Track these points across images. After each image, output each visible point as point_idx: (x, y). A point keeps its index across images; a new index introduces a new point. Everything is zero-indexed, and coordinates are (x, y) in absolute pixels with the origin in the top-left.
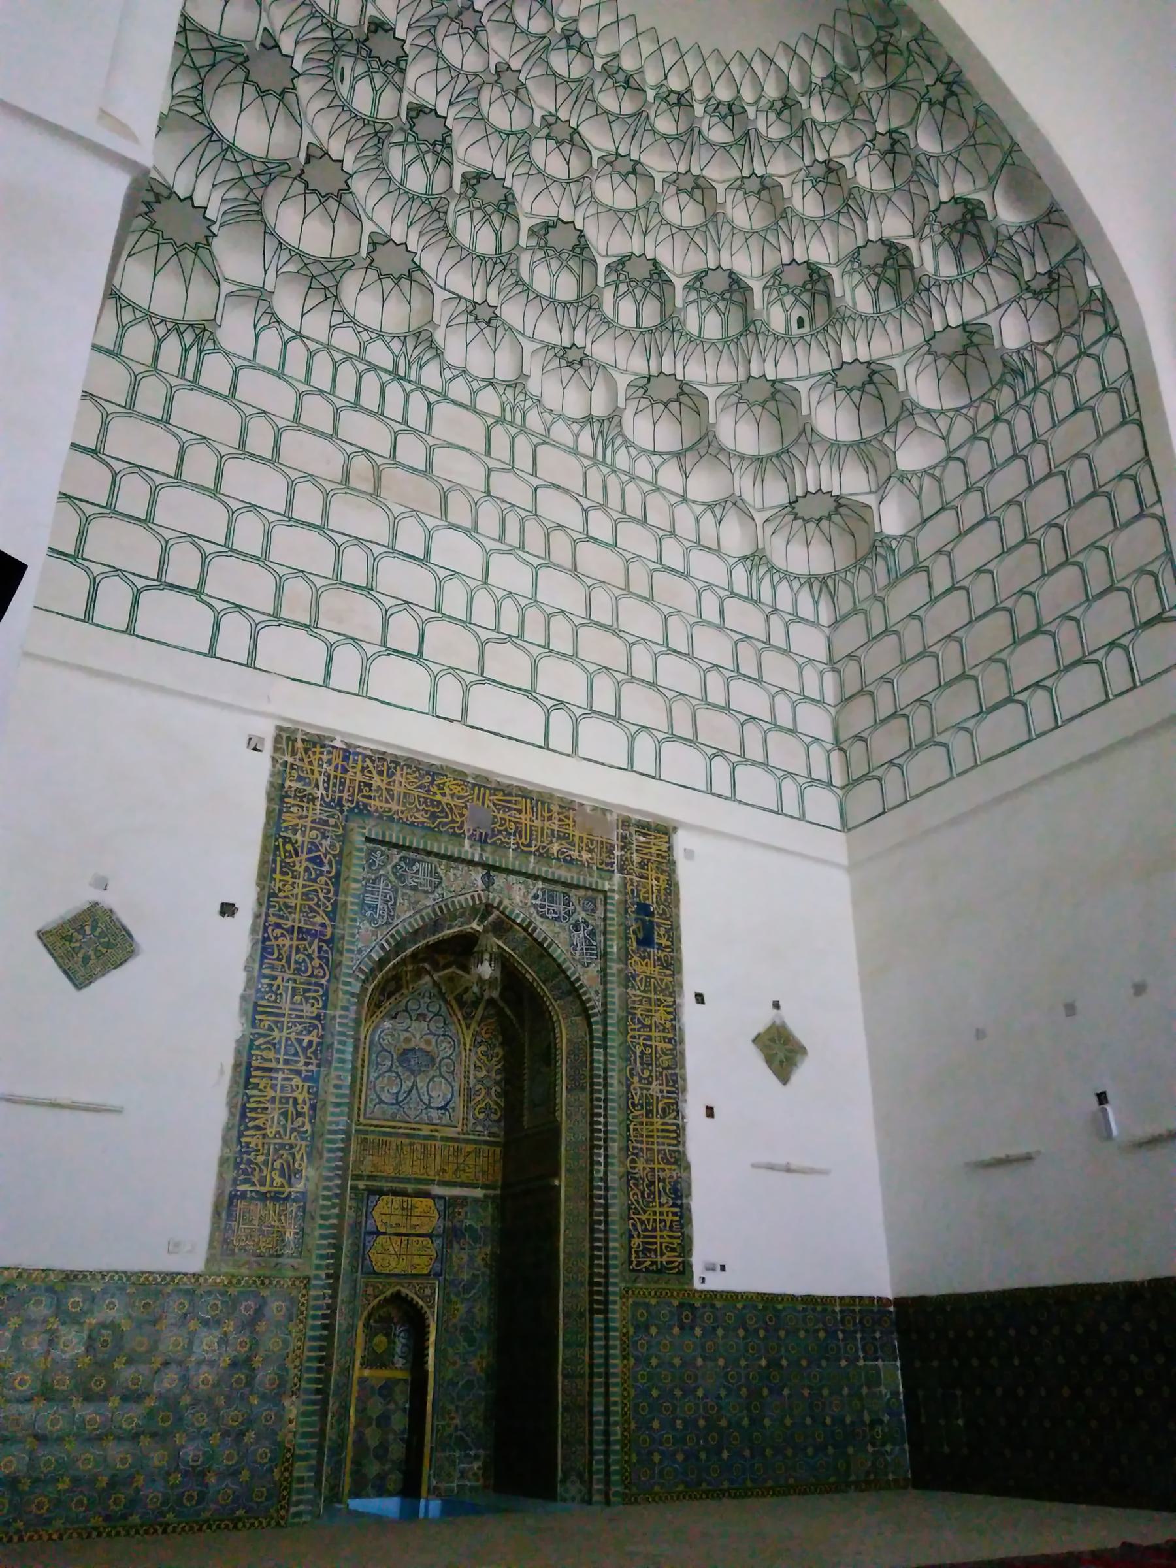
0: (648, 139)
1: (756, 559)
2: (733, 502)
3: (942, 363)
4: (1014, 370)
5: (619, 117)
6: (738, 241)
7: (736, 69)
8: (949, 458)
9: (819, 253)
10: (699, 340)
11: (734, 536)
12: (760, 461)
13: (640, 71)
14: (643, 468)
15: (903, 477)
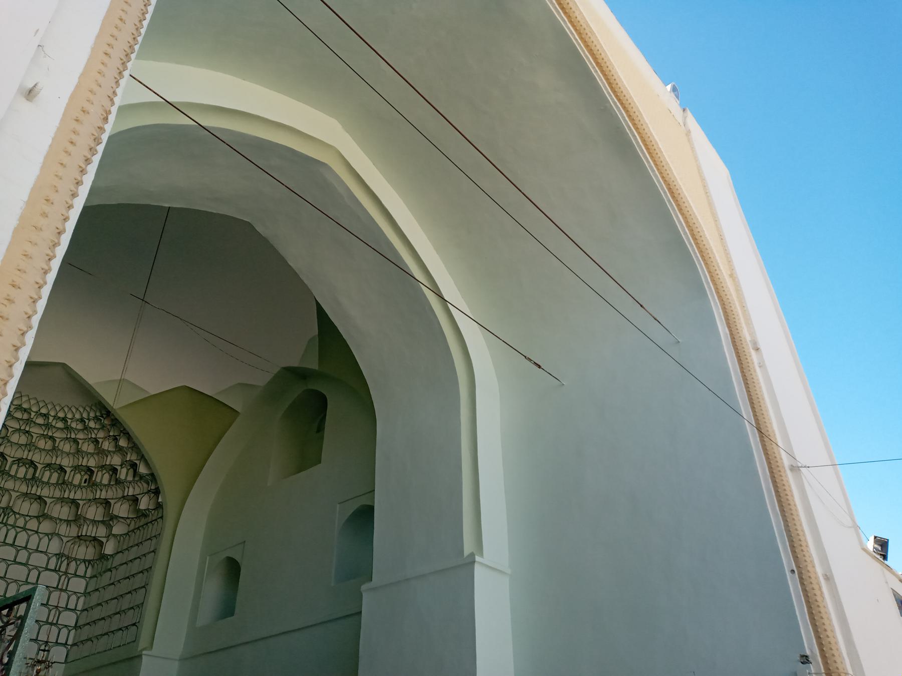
0: (32, 425)
1: (59, 556)
2: (58, 535)
3: (131, 502)
4: (143, 514)
5: (22, 419)
6: (64, 455)
7: (66, 409)
8: (127, 534)
9: (92, 463)
10: (48, 483)
11: (55, 546)
12: (68, 522)
13: (30, 409)
14: (21, 522)
15: (114, 535)
